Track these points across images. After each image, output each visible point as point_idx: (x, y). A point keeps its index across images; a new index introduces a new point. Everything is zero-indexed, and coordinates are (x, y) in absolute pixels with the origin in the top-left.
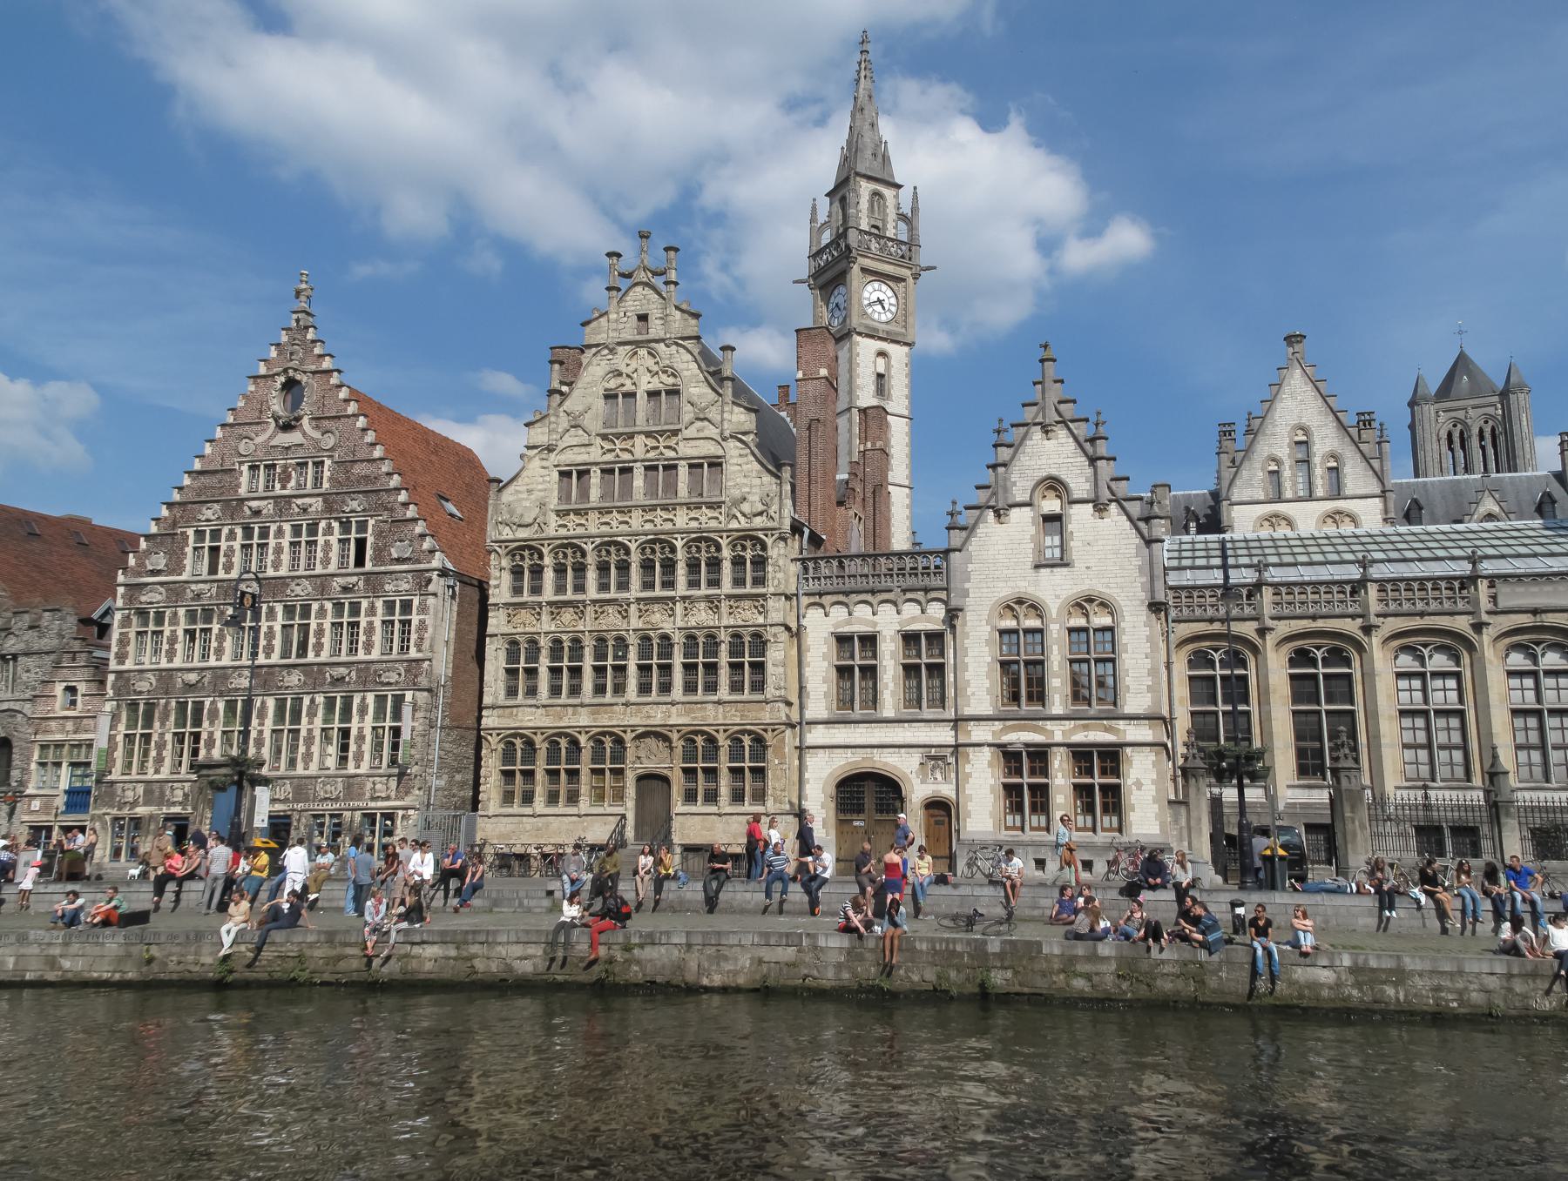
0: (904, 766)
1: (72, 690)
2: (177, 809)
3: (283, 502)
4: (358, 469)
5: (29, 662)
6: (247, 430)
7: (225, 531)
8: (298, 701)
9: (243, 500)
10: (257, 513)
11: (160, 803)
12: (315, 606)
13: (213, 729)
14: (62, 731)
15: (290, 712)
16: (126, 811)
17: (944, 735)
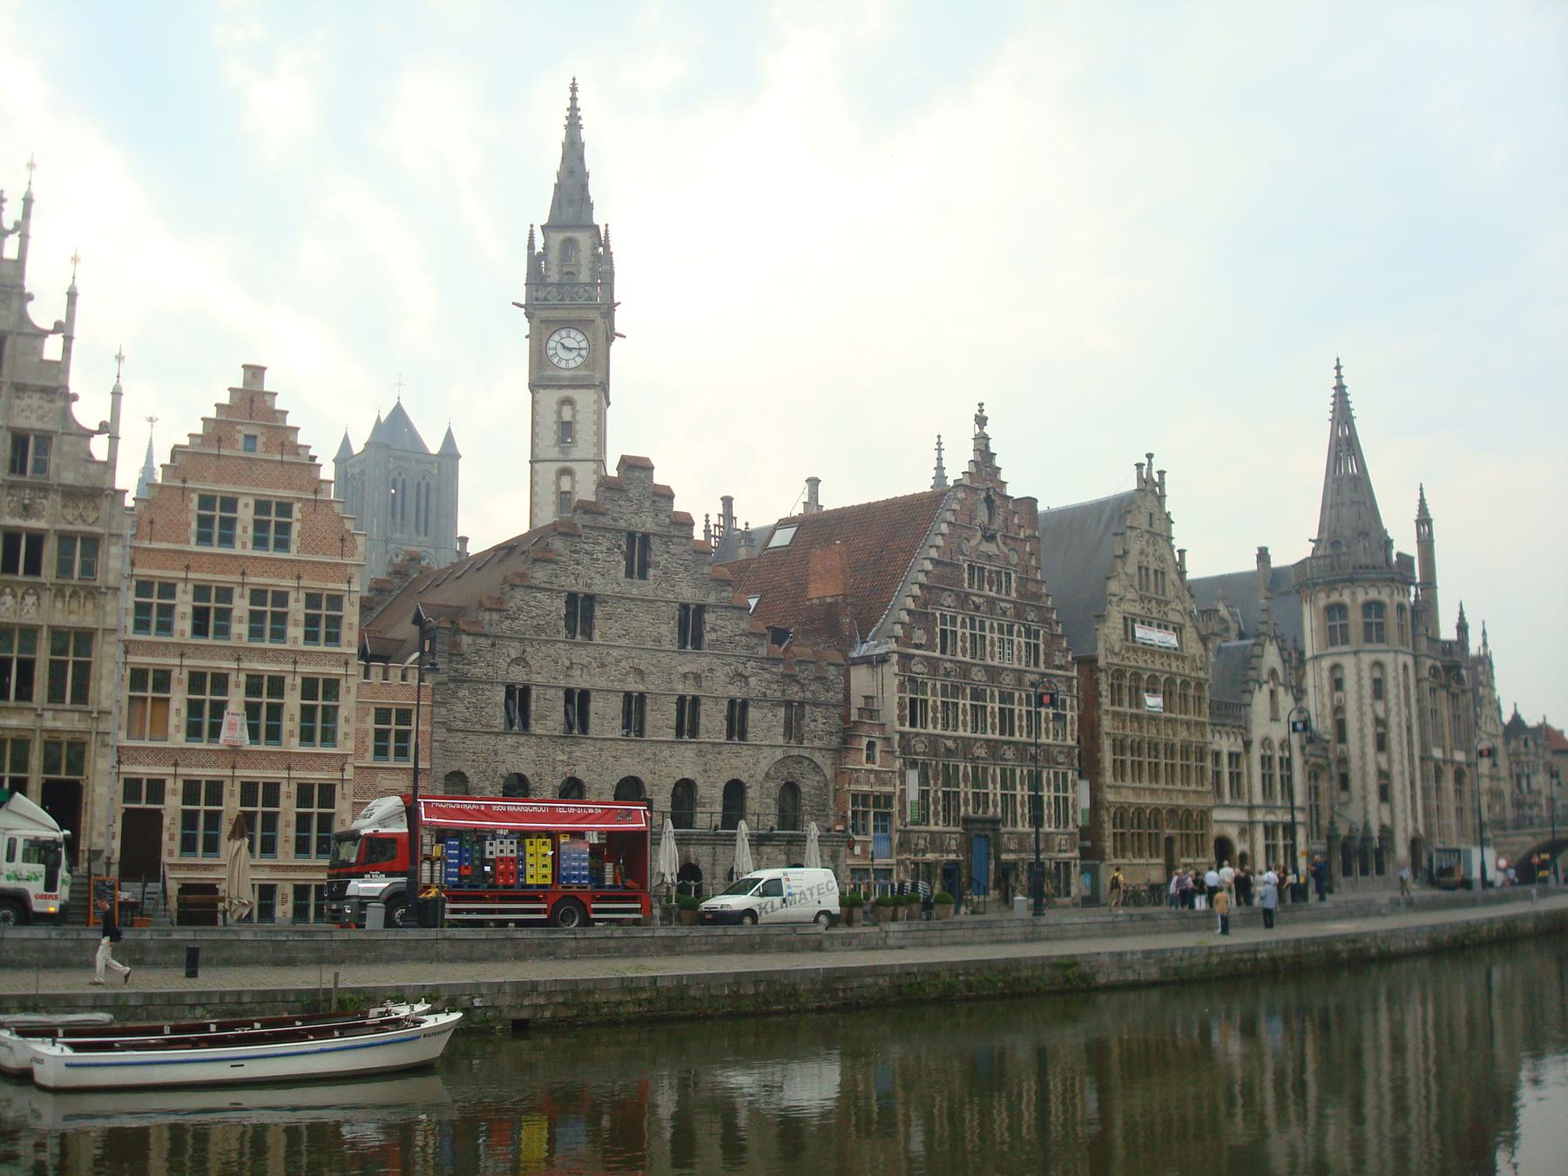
0: (1232, 832)
1: (871, 745)
2: (952, 857)
3: (991, 602)
4: (1031, 587)
5: (819, 713)
6: (966, 533)
7: (959, 619)
8: (1013, 772)
9: (968, 595)
10: (977, 608)
11: (943, 849)
12: (1017, 695)
13: (966, 790)
14: (868, 782)
15: (1007, 781)
16: (919, 857)
17: (1242, 816)
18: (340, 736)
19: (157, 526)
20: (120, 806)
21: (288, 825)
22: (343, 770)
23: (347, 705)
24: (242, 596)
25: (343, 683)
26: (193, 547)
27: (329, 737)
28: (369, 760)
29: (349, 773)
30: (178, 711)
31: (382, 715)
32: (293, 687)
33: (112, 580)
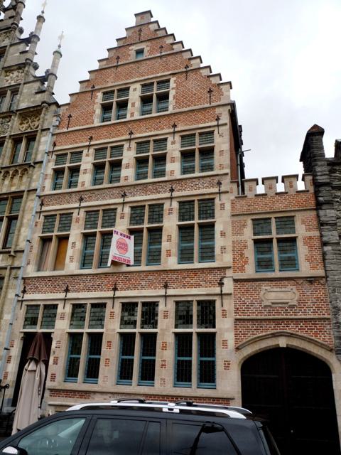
18: (217, 251)
19: (73, 118)
20: (20, 329)
21: (164, 347)
22: (221, 284)
23: (222, 220)
24: (129, 149)
25: (217, 202)
26: (97, 123)
27: (208, 254)
28: (250, 271)
29: (229, 286)
30: (74, 243)
31: (260, 224)
32: (171, 211)
33: (39, 159)
